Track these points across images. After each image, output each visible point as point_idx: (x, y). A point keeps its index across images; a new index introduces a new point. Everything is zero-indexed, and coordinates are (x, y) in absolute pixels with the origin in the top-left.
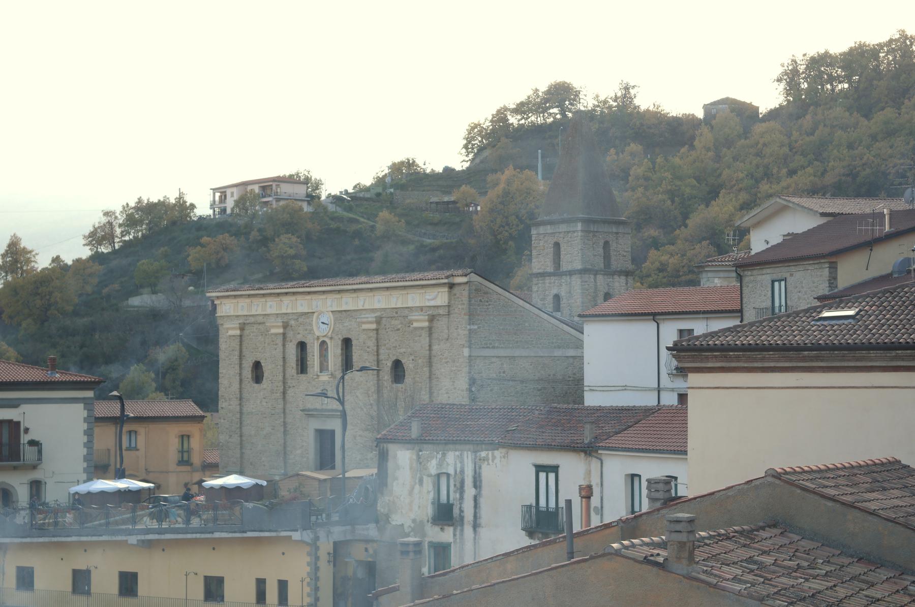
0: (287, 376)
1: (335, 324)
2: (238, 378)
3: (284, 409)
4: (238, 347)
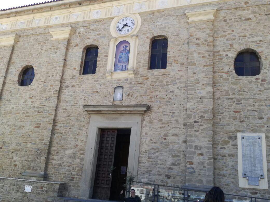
0: (67, 75)
1: (143, 24)
3: (57, 108)
4: (8, 55)
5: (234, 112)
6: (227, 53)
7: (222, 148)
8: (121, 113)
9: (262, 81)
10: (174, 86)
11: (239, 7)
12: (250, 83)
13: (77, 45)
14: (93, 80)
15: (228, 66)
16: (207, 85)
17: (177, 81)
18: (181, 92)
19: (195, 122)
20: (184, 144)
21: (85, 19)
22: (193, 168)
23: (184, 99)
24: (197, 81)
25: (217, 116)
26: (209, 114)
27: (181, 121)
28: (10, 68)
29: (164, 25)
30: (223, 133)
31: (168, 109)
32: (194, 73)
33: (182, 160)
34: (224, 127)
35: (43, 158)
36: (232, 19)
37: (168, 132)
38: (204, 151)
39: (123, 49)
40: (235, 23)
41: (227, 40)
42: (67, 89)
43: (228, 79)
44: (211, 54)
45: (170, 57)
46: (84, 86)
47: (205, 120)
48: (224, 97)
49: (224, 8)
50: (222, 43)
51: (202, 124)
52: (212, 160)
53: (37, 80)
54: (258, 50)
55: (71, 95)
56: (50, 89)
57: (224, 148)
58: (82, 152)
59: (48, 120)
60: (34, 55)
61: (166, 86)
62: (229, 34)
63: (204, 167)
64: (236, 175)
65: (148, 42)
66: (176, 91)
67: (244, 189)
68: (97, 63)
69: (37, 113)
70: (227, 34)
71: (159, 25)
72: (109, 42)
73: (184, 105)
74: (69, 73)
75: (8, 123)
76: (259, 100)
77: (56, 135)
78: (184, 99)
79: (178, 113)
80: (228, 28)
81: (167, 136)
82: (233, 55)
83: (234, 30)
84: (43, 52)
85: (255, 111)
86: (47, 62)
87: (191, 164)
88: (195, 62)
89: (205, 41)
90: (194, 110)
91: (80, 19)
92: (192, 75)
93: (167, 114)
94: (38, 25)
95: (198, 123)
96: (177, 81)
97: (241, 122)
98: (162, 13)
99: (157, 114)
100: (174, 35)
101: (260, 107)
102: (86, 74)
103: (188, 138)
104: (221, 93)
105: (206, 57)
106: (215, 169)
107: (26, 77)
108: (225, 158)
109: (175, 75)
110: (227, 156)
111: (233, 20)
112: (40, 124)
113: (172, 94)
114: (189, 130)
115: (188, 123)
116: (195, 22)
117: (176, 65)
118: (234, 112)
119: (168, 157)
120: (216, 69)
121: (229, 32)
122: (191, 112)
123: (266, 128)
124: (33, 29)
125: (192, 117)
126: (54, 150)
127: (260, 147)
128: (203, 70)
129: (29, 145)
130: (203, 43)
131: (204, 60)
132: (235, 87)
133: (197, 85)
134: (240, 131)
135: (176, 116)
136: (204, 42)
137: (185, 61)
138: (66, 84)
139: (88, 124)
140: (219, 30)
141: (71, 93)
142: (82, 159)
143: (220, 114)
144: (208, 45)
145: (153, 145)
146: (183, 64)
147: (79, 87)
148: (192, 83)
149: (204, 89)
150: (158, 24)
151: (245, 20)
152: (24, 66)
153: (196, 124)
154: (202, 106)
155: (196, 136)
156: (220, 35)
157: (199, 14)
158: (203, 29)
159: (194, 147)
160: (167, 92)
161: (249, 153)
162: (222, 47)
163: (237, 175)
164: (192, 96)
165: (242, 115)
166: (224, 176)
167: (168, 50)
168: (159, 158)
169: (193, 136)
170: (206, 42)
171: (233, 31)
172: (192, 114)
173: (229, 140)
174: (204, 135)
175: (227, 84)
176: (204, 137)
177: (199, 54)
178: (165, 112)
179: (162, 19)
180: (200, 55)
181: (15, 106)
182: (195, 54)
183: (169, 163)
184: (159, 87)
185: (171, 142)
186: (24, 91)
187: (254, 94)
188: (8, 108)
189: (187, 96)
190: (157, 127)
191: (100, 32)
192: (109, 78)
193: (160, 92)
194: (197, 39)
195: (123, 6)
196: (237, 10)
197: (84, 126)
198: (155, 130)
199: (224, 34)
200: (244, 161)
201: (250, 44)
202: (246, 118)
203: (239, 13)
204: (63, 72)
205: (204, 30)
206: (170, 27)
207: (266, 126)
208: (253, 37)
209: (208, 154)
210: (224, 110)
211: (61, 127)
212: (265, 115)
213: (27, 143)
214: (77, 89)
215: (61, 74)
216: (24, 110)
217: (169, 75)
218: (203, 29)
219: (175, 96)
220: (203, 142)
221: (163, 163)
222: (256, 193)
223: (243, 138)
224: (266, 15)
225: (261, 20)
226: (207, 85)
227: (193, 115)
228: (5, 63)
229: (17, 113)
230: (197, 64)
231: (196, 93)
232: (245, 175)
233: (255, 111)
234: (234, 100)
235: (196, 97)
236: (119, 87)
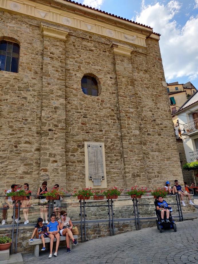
6: (76, 73)
7: (72, 155)
9: (101, 101)
10: (27, 92)
11: (85, 38)
12: (93, 101)
17: (31, 89)
18: (34, 100)
19: (50, 130)
20: (36, 152)
22: (48, 175)
23: (38, 107)
25: (68, 127)
26: (62, 123)
27: (34, 129)
29: (15, 29)
30: (73, 141)
31: (20, 115)
32: (49, 84)
33: (34, 168)
34: (74, 136)
36: (79, 46)
37: (19, 139)
38: (58, 158)
40: (82, 50)
41: (76, 62)
43: (77, 96)
47: (59, 129)
48: (74, 110)
49: (73, 34)
50: (71, 63)
51: (56, 132)
52: (65, 167)
54: (99, 76)
61: (19, 92)
63: (58, 173)
64: (83, 179)
66: (29, 98)
70: (76, 57)
73: (38, 113)
76: (100, 116)
79: (31, 120)
80: (76, 52)
81: (19, 144)
82: (80, 75)
83: (82, 56)
85: (97, 124)
87: (45, 171)
88: (50, 73)
90: (49, 119)
92: (46, 85)
93: (19, 121)
95: (52, 131)
96: (31, 89)
97: (87, 133)
98: (14, 16)
99: (7, 119)
100: (27, 42)
101: (100, 122)
104: (71, 106)
105: (59, 71)
108: (74, 164)
109: (29, 82)
110: (76, 162)
111: (80, 47)
113: (25, 100)
114: (44, 137)
115: (43, 130)
116: (50, 37)
117: (29, 72)
119: (19, 166)
121: (78, 56)
122: (45, 120)
123: (104, 139)
125: (47, 125)
127: (101, 153)
128: (57, 82)
130: (57, 59)
131: (57, 74)
132: (82, 103)
133: (52, 95)
134: (86, 141)
135: (29, 123)
136: (57, 58)
137: (38, 70)
140: (69, 52)
143: (70, 125)
144: (61, 61)
146: (36, 73)
148: (46, 93)
149: (58, 100)
150: (8, 24)
151: (89, 50)
153: (50, 132)
154: (56, 115)
155: (50, 144)
156: (70, 56)
157: (53, 30)
158: (56, 46)
159: (48, 155)
160: (20, 98)
161: (93, 158)
162: (72, 66)
164: (46, 105)
165: (87, 127)
166: (74, 180)
167: (21, 55)
169: (48, 143)
170: (59, 59)
172: (46, 123)
173: (78, 148)
174: (58, 143)
177: (53, 67)
178: (16, 118)
179: (14, 22)
180: (53, 69)
184: (10, 91)
185: (23, 150)
189: (42, 105)
190: (7, 133)
194: (51, 53)
196: (83, 40)
198: (4, 136)
199: (74, 56)
201: (93, 70)
202: (90, 129)
203: (85, 43)
205: (58, 47)
206: (23, 34)
207: (104, 137)
209: (62, 161)
210: (74, 121)
217: (22, 80)
218: (56, 46)
219: (28, 103)
220: (57, 149)
221: (14, 172)
223: (89, 146)
224: (104, 51)
227: (48, 123)
231: (50, 102)
232: (91, 177)
233: (97, 124)
235: (51, 106)
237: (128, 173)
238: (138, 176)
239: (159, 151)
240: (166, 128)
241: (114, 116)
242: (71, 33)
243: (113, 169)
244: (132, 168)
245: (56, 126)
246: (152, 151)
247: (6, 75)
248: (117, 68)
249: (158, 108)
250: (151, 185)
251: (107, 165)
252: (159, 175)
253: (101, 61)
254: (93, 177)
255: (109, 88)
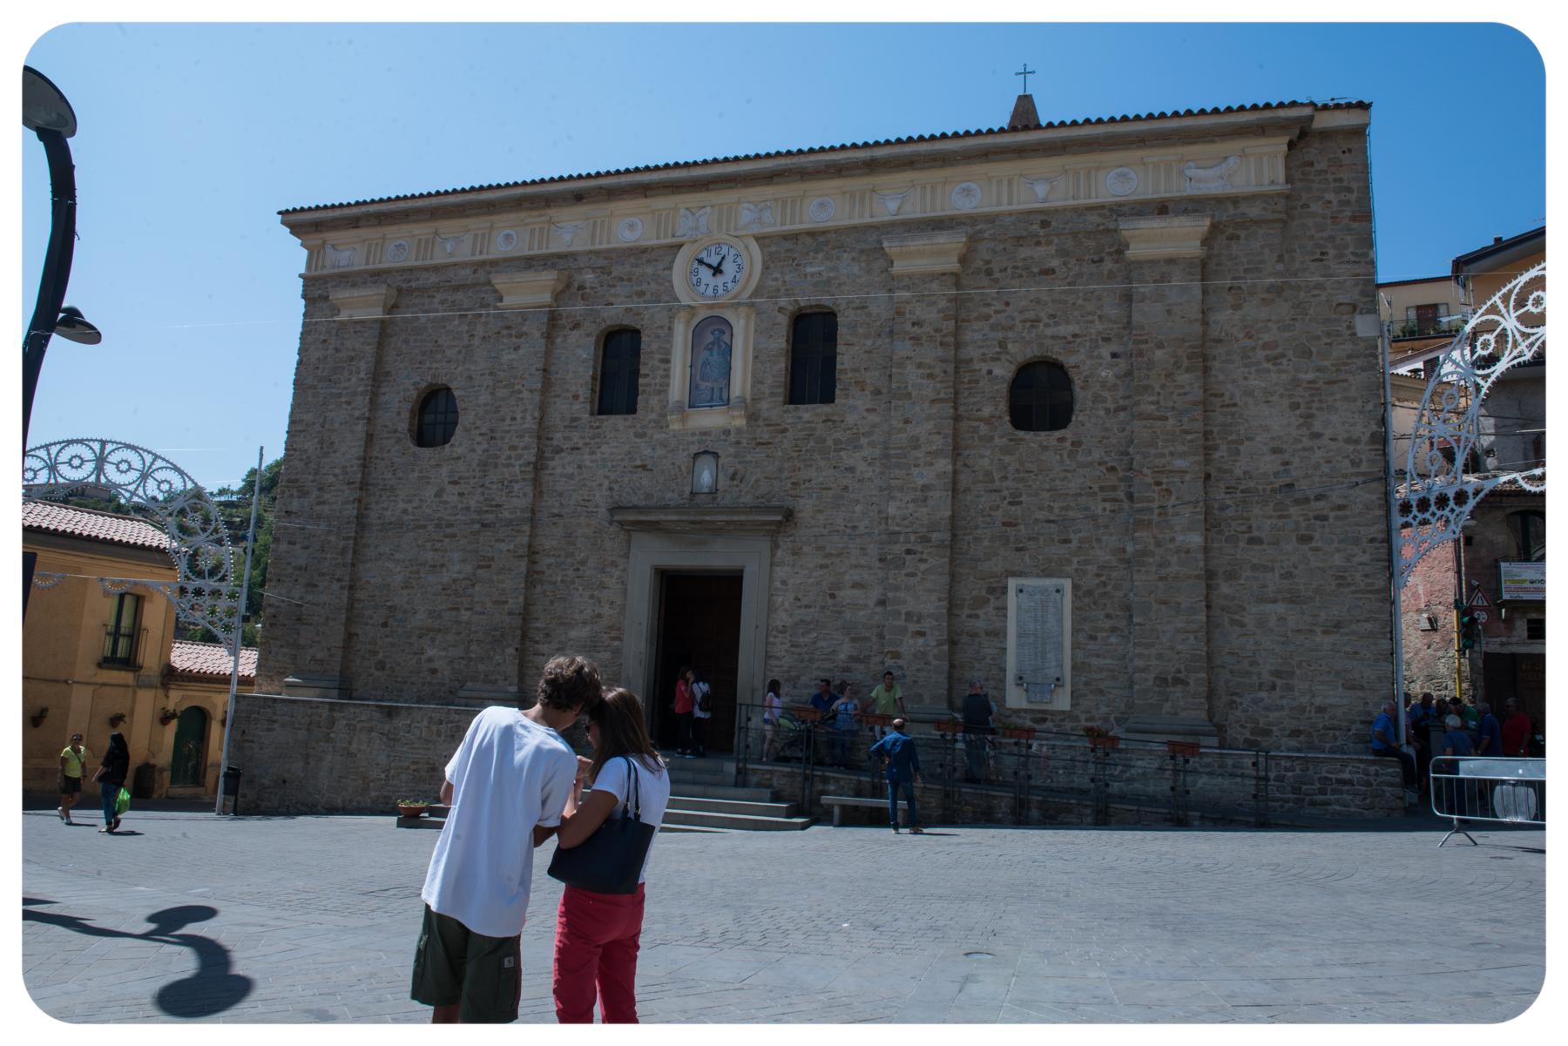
1: (766, 268)
2: (360, 428)
4: (370, 350)
5: (1004, 524)
7: (969, 616)
8: (717, 531)
9: (1073, 444)
12: (1045, 448)
13: (576, 326)
14: (631, 431)
15: (992, 403)
16: (937, 454)
19: (908, 552)
20: (878, 609)
21: (597, 247)
22: (901, 668)
24: (915, 443)
28: (383, 390)
32: (907, 422)
35: (511, 651)
38: (927, 624)
39: (710, 338)
41: (993, 328)
42: (557, 457)
43: (992, 438)
44: (951, 368)
45: (844, 371)
46: (604, 448)
50: (978, 336)
53: (467, 430)
54: (1069, 361)
55: (571, 476)
56: (510, 457)
57: (977, 616)
58: (614, 633)
59: (512, 547)
60: (449, 353)
62: (997, 312)
65: (784, 321)
66: (861, 467)
67: (1017, 712)
68: (641, 380)
69: (477, 526)
71: (812, 275)
72: (671, 319)
74: (562, 409)
75: (397, 556)
77: (539, 588)
78: (881, 490)
82: (1004, 371)
84: (476, 342)
86: (491, 374)
89: (936, 330)
91: (579, 246)
92: (901, 425)
94: (455, 260)
96: (864, 441)
97: (1018, 550)
98: (821, 239)
102: (610, 412)
103: (890, 595)
106: (952, 666)
107: (429, 418)
112: (492, 559)
118: (1004, 524)
120: (962, 408)
121: (998, 306)
123: (1075, 566)
124: (436, 269)
126: (538, 629)
129: (465, 616)
132: (1007, 459)
134: (1014, 574)
135: (861, 535)
138: (555, 442)
139: (626, 556)
141: (569, 470)
142: (617, 652)
145: (803, 611)
147: (593, 453)
150: (809, 270)
152: (424, 385)
156: (974, 315)
163: (1003, 681)
168: (820, 644)
171: (1007, 304)
175: (988, 453)
176: (930, 591)
177: (919, 366)
179: (820, 256)
181: (410, 507)
182: (910, 368)
183: (842, 656)
186: (432, 462)
187: (1053, 480)
188: (388, 513)
191: (644, 287)
192: (675, 426)
193: (819, 469)
194: (914, 324)
195: (708, 209)
197: (613, 564)
199: (985, 310)
200: (1020, 645)
201: (1049, 342)
203: (1024, 252)
204: (543, 408)
207: (1075, 560)
208: (1057, 324)
211: (549, 566)
212: (1075, 532)
213: (458, 609)
214: (587, 457)
215: (537, 414)
216: (440, 519)
222: (1045, 720)
225: (1080, 275)
226: (937, 454)
228: (362, 375)
229: (419, 527)
230: (914, 393)
234: (1006, 493)
236: (706, 452)
237: (1143, 670)
238: (1177, 681)
239: (1294, 599)
240: (1340, 513)
241: (1114, 488)
242: (980, 232)
243: (1098, 656)
244: (1160, 657)
245: (925, 540)
246: (1261, 600)
247: (806, 416)
248: (1137, 318)
249: (1317, 436)
250: (1238, 713)
251: (1075, 646)
252: (1279, 682)
253: (1080, 302)
254: (1028, 678)
255: (1106, 394)
